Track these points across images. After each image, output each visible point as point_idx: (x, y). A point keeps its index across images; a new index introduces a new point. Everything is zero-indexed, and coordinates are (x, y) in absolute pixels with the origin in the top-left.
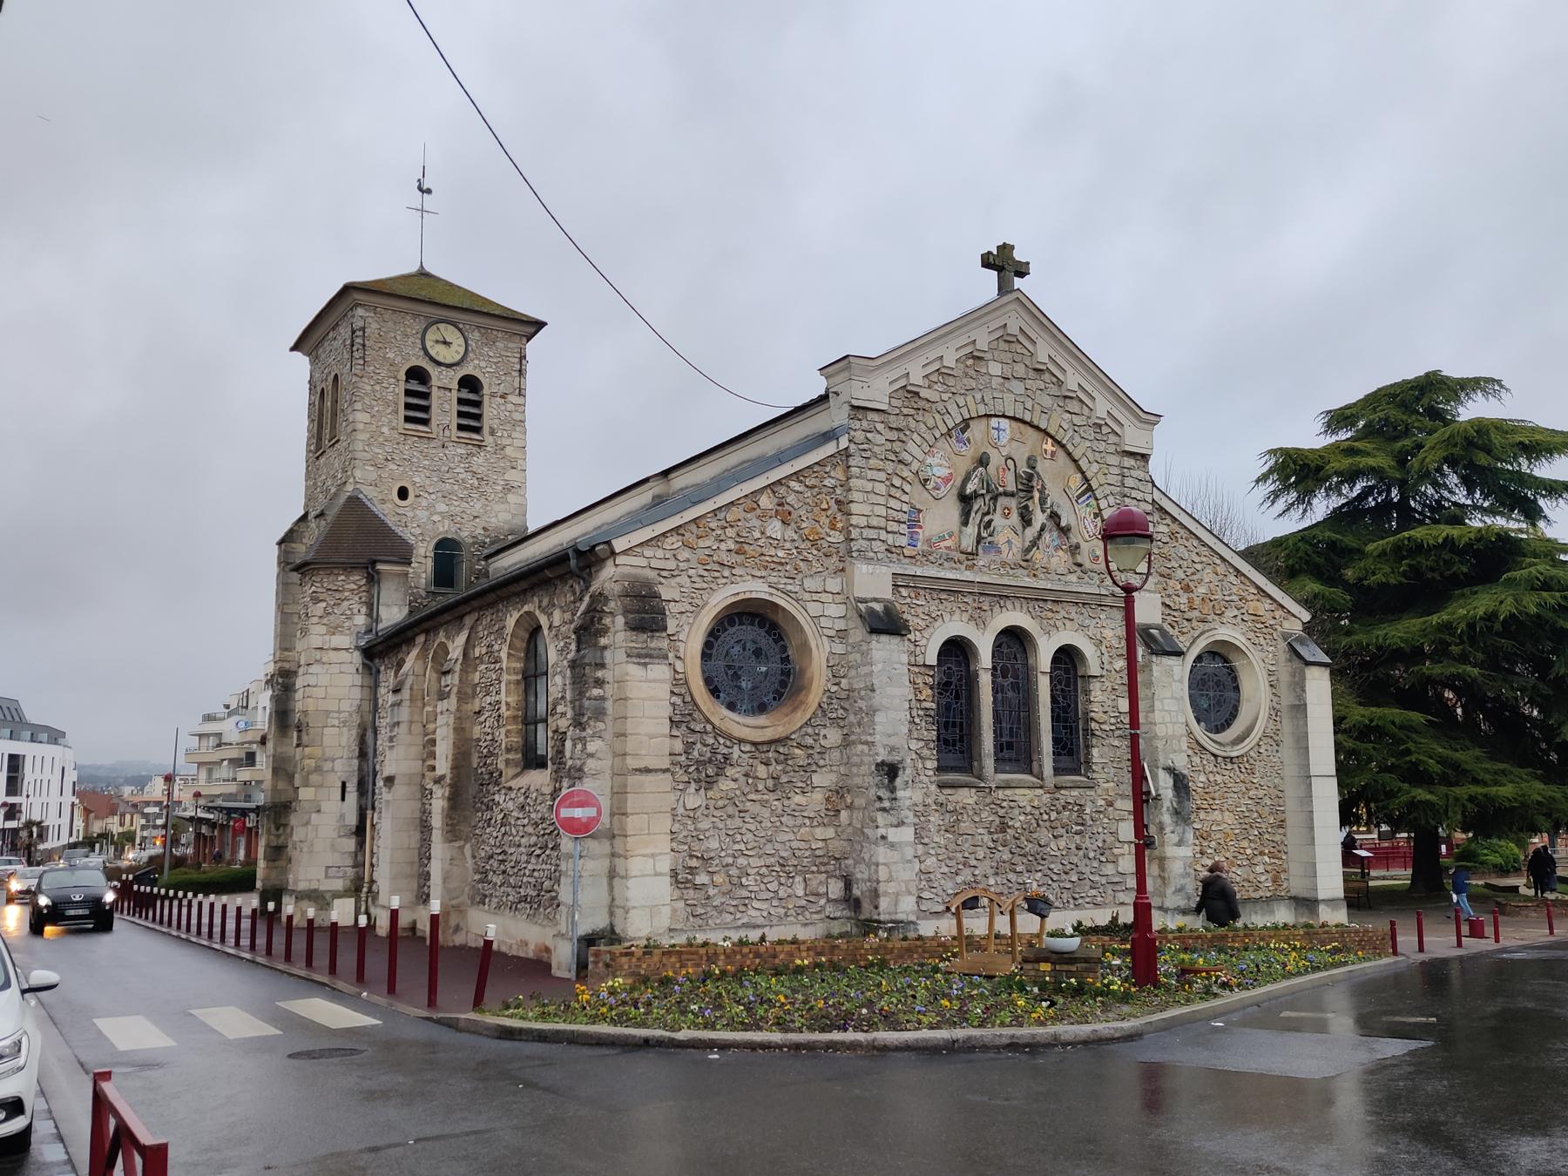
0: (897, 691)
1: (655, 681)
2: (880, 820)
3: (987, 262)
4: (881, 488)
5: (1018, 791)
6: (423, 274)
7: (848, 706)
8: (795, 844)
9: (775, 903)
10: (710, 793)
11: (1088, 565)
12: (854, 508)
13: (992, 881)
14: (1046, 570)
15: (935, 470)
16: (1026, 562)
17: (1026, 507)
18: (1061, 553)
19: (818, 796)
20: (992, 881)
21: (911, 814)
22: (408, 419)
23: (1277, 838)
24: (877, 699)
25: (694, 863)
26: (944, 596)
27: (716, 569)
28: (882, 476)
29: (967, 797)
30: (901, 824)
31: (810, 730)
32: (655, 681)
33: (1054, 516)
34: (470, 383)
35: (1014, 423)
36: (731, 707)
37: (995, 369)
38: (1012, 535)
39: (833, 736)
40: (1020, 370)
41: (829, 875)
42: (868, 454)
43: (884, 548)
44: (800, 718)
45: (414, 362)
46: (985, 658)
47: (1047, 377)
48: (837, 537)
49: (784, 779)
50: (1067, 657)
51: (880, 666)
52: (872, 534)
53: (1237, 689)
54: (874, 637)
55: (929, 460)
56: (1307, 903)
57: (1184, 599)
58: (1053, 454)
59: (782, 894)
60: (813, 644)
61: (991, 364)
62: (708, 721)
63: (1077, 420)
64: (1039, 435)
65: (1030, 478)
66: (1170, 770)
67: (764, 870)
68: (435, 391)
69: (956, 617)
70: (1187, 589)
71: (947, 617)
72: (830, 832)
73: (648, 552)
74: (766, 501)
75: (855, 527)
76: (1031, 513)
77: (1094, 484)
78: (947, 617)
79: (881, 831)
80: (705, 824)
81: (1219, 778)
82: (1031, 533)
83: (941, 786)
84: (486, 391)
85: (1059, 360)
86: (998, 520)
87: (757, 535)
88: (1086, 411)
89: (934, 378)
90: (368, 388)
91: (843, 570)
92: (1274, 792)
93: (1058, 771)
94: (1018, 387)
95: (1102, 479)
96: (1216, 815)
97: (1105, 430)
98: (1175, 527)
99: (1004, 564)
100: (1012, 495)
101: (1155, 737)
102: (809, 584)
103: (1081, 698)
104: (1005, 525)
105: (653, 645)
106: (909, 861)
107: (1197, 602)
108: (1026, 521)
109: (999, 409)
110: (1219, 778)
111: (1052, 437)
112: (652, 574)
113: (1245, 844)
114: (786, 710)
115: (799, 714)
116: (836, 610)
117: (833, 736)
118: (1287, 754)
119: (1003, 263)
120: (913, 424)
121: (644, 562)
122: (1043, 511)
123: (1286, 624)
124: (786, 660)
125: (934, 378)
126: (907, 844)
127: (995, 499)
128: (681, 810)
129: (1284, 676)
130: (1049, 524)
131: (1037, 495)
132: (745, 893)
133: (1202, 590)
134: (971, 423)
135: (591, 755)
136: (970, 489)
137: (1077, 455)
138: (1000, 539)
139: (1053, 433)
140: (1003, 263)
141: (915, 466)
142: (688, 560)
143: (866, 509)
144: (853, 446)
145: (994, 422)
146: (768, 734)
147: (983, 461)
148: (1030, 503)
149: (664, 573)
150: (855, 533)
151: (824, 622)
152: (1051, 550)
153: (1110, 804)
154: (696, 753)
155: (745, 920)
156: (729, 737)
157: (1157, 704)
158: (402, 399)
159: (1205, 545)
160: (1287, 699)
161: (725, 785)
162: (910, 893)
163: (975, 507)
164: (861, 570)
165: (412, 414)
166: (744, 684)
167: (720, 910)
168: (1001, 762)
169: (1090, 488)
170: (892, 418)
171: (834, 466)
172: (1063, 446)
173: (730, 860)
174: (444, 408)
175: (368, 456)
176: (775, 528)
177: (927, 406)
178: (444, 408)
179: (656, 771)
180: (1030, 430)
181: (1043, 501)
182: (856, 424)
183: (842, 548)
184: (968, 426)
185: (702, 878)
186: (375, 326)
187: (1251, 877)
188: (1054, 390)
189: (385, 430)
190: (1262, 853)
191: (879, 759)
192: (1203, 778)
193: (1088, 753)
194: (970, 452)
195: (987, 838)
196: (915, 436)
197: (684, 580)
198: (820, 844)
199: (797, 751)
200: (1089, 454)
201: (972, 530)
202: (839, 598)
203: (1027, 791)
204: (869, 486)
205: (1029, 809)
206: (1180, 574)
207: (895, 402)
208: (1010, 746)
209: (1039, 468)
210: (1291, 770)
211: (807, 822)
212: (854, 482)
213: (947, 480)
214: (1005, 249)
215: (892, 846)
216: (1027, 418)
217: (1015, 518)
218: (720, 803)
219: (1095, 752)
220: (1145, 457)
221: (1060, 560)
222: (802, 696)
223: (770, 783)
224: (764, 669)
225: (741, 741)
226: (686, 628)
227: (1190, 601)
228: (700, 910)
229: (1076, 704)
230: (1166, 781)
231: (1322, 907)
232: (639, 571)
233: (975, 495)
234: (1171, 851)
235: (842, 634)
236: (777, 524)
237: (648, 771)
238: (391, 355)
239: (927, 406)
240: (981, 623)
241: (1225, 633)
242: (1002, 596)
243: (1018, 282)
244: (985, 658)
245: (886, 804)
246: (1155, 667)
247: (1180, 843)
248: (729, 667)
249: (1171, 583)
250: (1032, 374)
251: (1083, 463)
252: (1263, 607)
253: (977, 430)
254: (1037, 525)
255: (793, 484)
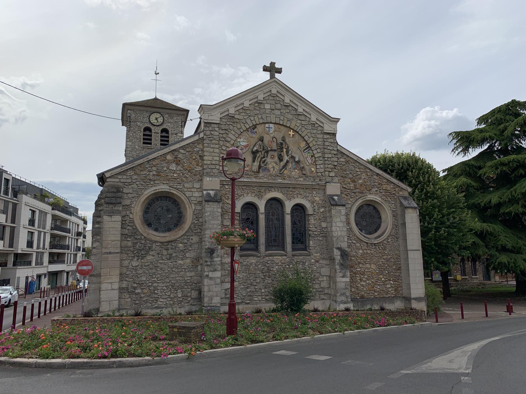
0: (216, 222)
1: (115, 221)
2: (206, 269)
3: (265, 69)
4: (217, 151)
5: (275, 257)
6: (156, 99)
7: (199, 227)
8: (177, 278)
9: (169, 299)
10: (142, 261)
11: (308, 174)
12: (205, 158)
13: (263, 291)
14: (289, 177)
15: (241, 143)
16: (281, 174)
17: (281, 155)
18: (296, 170)
19: (188, 261)
20: (263, 291)
21: (220, 267)
22: (144, 143)
23: (397, 274)
24: (207, 226)
25: (135, 285)
26: (244, 188)
27: (147, 182)
28: (217, 146)
29: (253, 260)
30: (215, 270)
31: (185, 237)
32: (115, 221)
33: (293, 157)
34: (165, 131)
35: (276, 125)
36: (156, 230)
37: (267, 106)
38: (275, 165)
39: (195, 239)
40: (278, 106)
41: (192, 289)
42: (212, 139)
43: (217, 172)
44: (181, 233)
45: (146, 125)
46: (262, 208)
47: (290, 108)
48: (199, 168)
49: (174, 255)
50: (299, 208)
51: (208, 213)
52: (213, 167)
53: (380, 218)
54: (206, 203)
55: (239, 140)
56: (408, 299)
57: (352, 185)
58: (293, 135)
59: (171, 296)
60: (187, 206)
61: (266, 105)
62: (142, 235)
63: (303, 123)
64: (285, 128)
65: (282, 144)
66: (339, 249)
67: (165, 288)
68: (153, 134)
69: (249, 195)
70: (354, 181)
71: (245, 195)
72: (193, 274)
73: (119, 177)
74: (169, 157)
75: (205, 164)
76: (282, 157)
77: (311, 145)
78: (245, 195)
79: (207, 273)
80: (140, 272)
81: (369, 252)
82: (282, 164)
83: (241, 256)
84: (170, 133)
85: (294, 101)
86: (269, 160)
87: (165, 169)
88: (308, 119)
89: (241, 111)
90: (131, 134)
91: (201, 180)
92: (395, 257)
93: (294, 249)
94: (278, 112)
95: (314, 143)
96: (368, 266)
97: (316, 125)
98: (348, 159)
99: (271, 175)
100: (275, 150)
101: (333, 236)
102: (186, 185)
103: (307, 222)
104: (272, 163)
105: (115, 209)
106: (218, 284)
107: (358, 186)
108: (281, 159)
109: (269, 120)
110: (369, 252)
111: (293, 129)
112: (121, 184)
113: (381, 276)
114: (176, 230)
115: (180, 231)
116: (197, 194)
117: (195, 239)
118: (401, 241)
119: (272, 69)
120: (231, 127)
121: (118, 180)
122: (288, 156)
123: (401, 193)
124: (180, 213)
125: (241, 111)
126: (218, 278)
127: (267, 152)
128: (131, 267)
129: (399, 213)
130: (291, 161)
131: (285, 150)
132: (156, 296)
133: (360, 181)
134: (257, 126)
135: (94, 248)
136: (255, 148)
137: (303, 135)
138: (270, 166)
139: (293, 128)
140: (272, 69)
141: (232, 142)
142: (136, 179)
143: (210, 158)
144: (205, 136)
145: (267, 125)
146: (168, 239)
147: (261, 139)
148: (282, 153)
149: (126, 184)
150: (205, 167)
151: (192, 199)
152: (292, 170)
153: (318, 262)
154: (137, 246)
155: (156, 306)
156: (151, 241)
157: (334, 224)
158: (142, 137)
159: (362, 165)
160: (400, 222)
161: (149, 258)
162: (217, 296)
163: (258, 155)
164: (207, 179)
165: (150, 142)
166: (162, 222)
167: (146, 302)
168: (268, 246)
169: (309, 147)
170: (223, 126)
171: (198, 144)
172: (298, 132)
173: (150, 284)
174: (156, 139)
175: (131, 155)
176: (173, 167)
177: (238, 121)
178: (156, 139)
179: (113, 253)
180: (283, 127)
181: (287, 152)
182: (207, 129)
183: (201, 172)
184: (256, 127)
185: (139, 291)
186: (134, 115)
187: (384, 290)
188: (294, 112)
189: (137, 147)
190: (390, 280)
191: (207, 247)
192: (361, 252)
193: (309, 243)
194: (256, 136)
195: (261, 275)
196: (232, 132)
197: (134, 186)
198: (189, 278)
199: (180, 245)
200: (309, 134)
201: (256, 164)
202: (199, 190)
203: (279, 257)
204: (212, 150)
205: (280, 264)
206: (351, 176)
207: (223, 120)
208: (275, 240)
209: (287, 141)
210: (402, 248)
211: (184, 270)
212: (205, 149)
213: (246, 147)
214: (273, 64)
215: (211, 279)
216: (281, 123)
217: (276, 159)
218: (147, 264)
219: (311, 242)
220: (334, 135)
221: (296, 173)
222: (183, 225)
223: (168, 256)
224: (170, 216)
225: (156, 242)
226: (135, 202)
227: (355, 186)
228: (137, 302)
229: (305, 224)
230: (337, 254)
231: (412, 301)
232: (116, 183)
233: (257, 151)
234: (339, 279)
235: (200, 203)
236: (174, 165)
237: (110, 253)
238: (139, 124)
239: (238, 121)
240: (260, 197)
241: (370, 197)
242: (270, 187)
243: (277, 75)
244: (262, 208)
245: (209, 263)
246: (333, 211)
247: (343, 277)
248: (156, 216)
249: (346, 179)
250: (283, 107)
251: (306, 138)
252: (389, 187)
253: (259, 129)
254: (285, 161)
255: (181, 151)
